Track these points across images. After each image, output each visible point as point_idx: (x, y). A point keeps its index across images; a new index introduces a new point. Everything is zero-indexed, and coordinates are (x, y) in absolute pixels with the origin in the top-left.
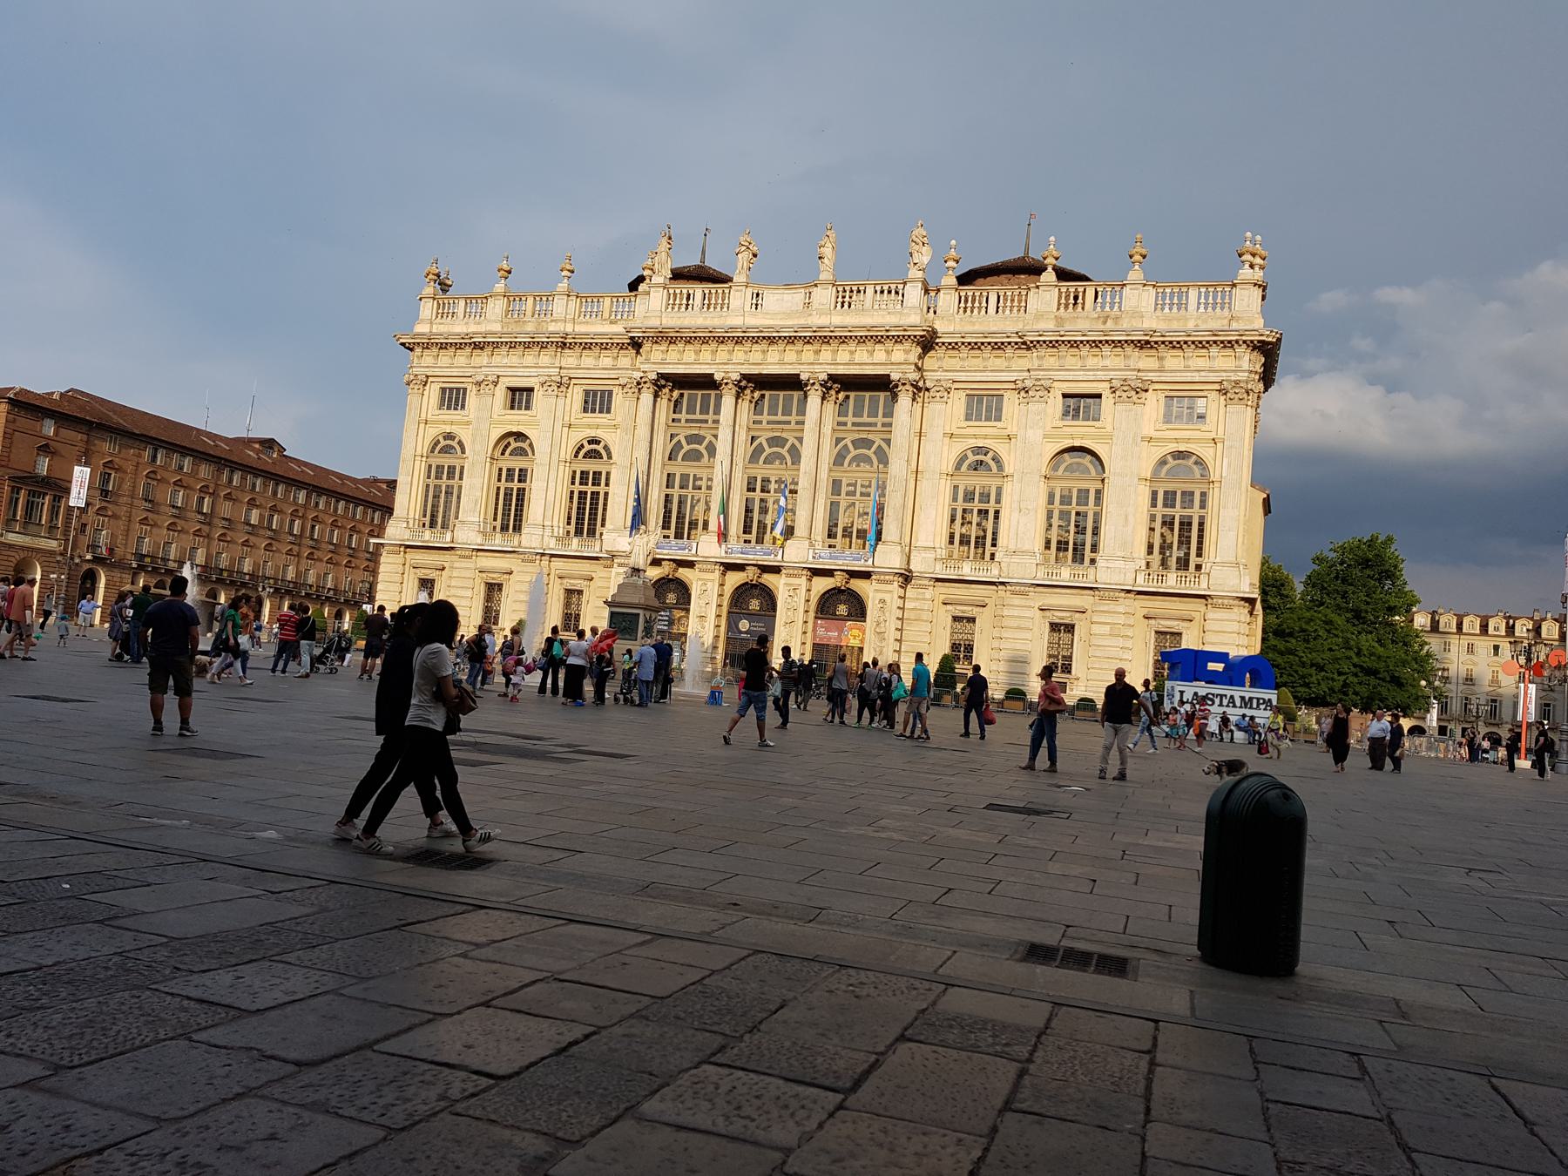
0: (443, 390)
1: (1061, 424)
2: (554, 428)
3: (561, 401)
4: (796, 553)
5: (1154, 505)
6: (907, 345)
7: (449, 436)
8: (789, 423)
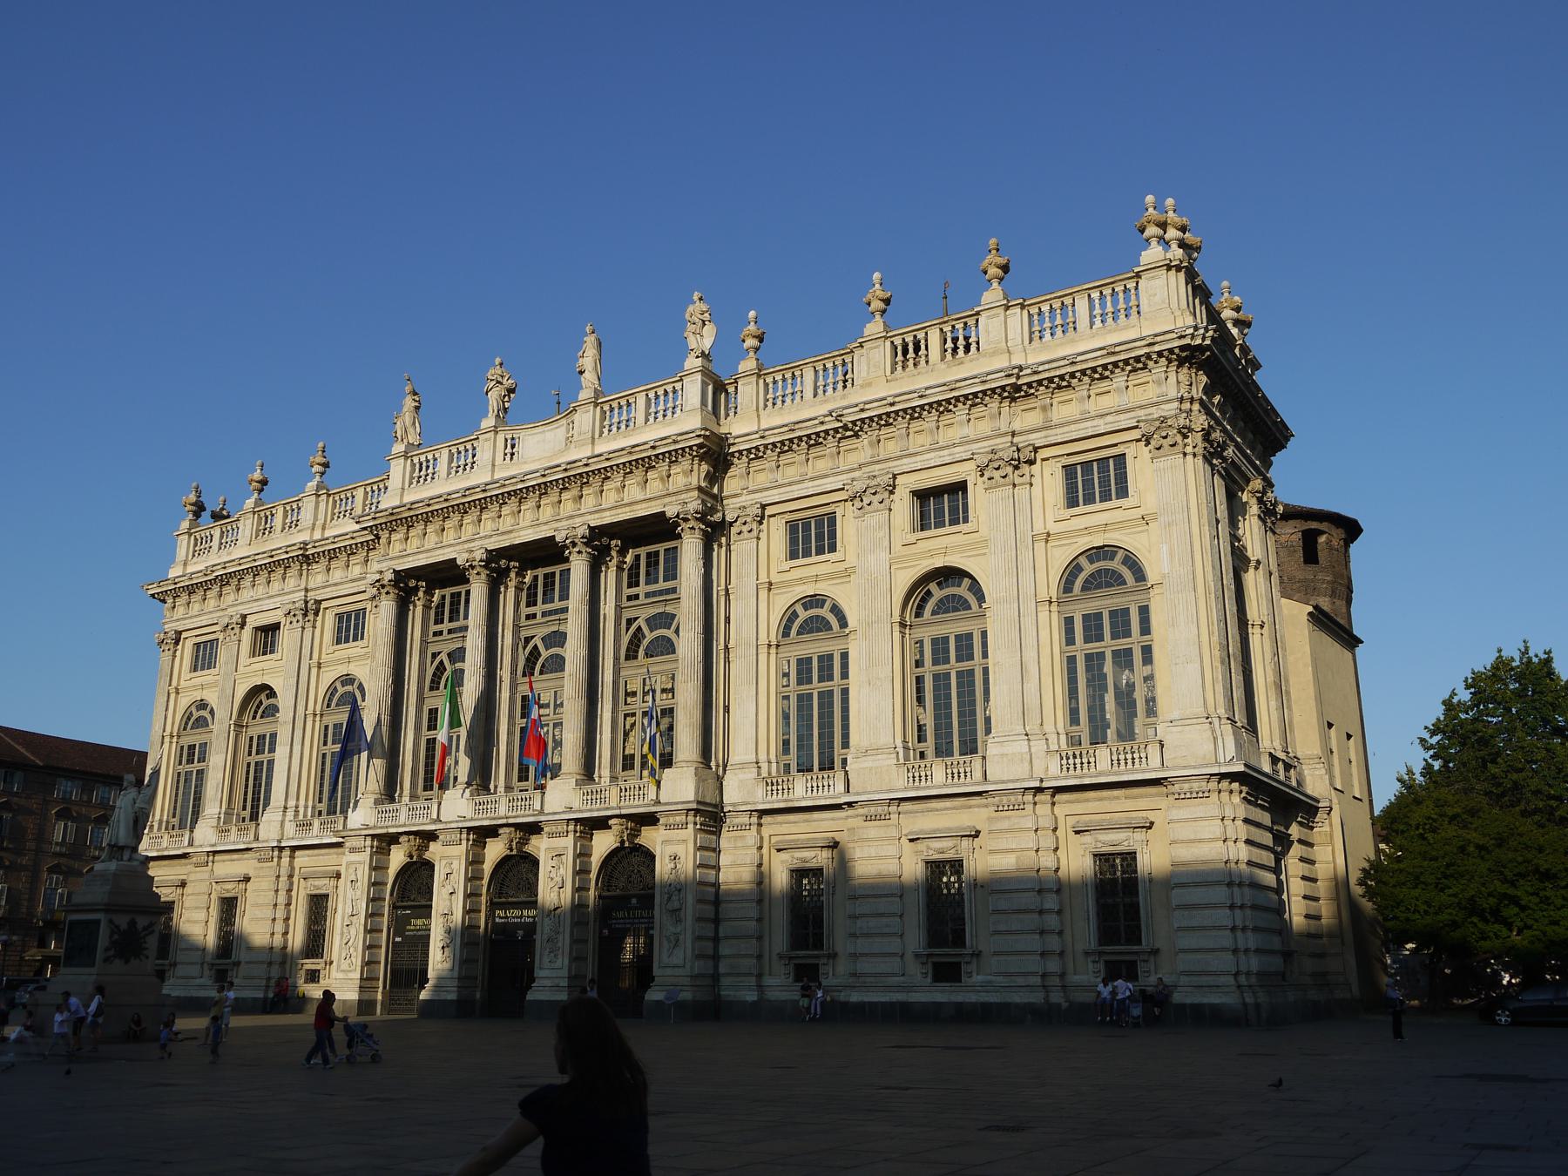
1: (912, 538)
3: (308, 632)
5: (1070, 641)
6: (685, 463)
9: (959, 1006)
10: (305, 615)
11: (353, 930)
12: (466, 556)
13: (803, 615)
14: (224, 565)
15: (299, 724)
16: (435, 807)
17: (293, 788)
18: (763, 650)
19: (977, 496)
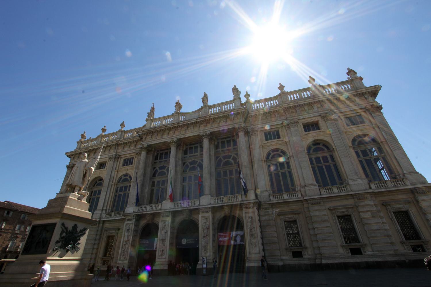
1: (306, 133)
3: (116, 162)
4: (206, 201)
8: (197, 155)
9: (367, 263)
10: (115, 159)
11: (127, 246)
12: (170, 140)
13: (272, 154)
15: (110, 186)
16: (160, 206)
17: (106, 204)
18: (264, 162)
19: (321, 123)
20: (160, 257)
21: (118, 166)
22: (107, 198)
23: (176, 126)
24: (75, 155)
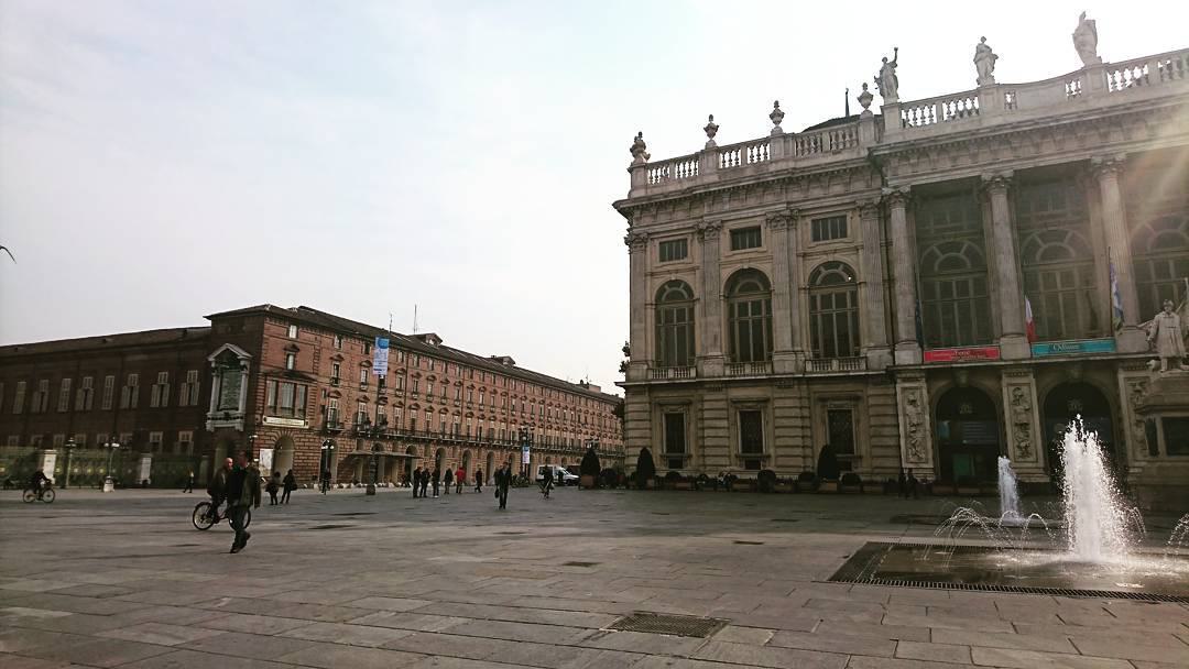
0: (660, 243)
2: (783, 260)
3: (792, 234)
7: (677, 283)
10: (788, 221)
11: (919, 436)
14: (709, 185)
17: (797, 338)
20: (1020, 459)
21: (800, 238)
22: (796, 323)
23: (1006, 134)
24: (644, 209)
